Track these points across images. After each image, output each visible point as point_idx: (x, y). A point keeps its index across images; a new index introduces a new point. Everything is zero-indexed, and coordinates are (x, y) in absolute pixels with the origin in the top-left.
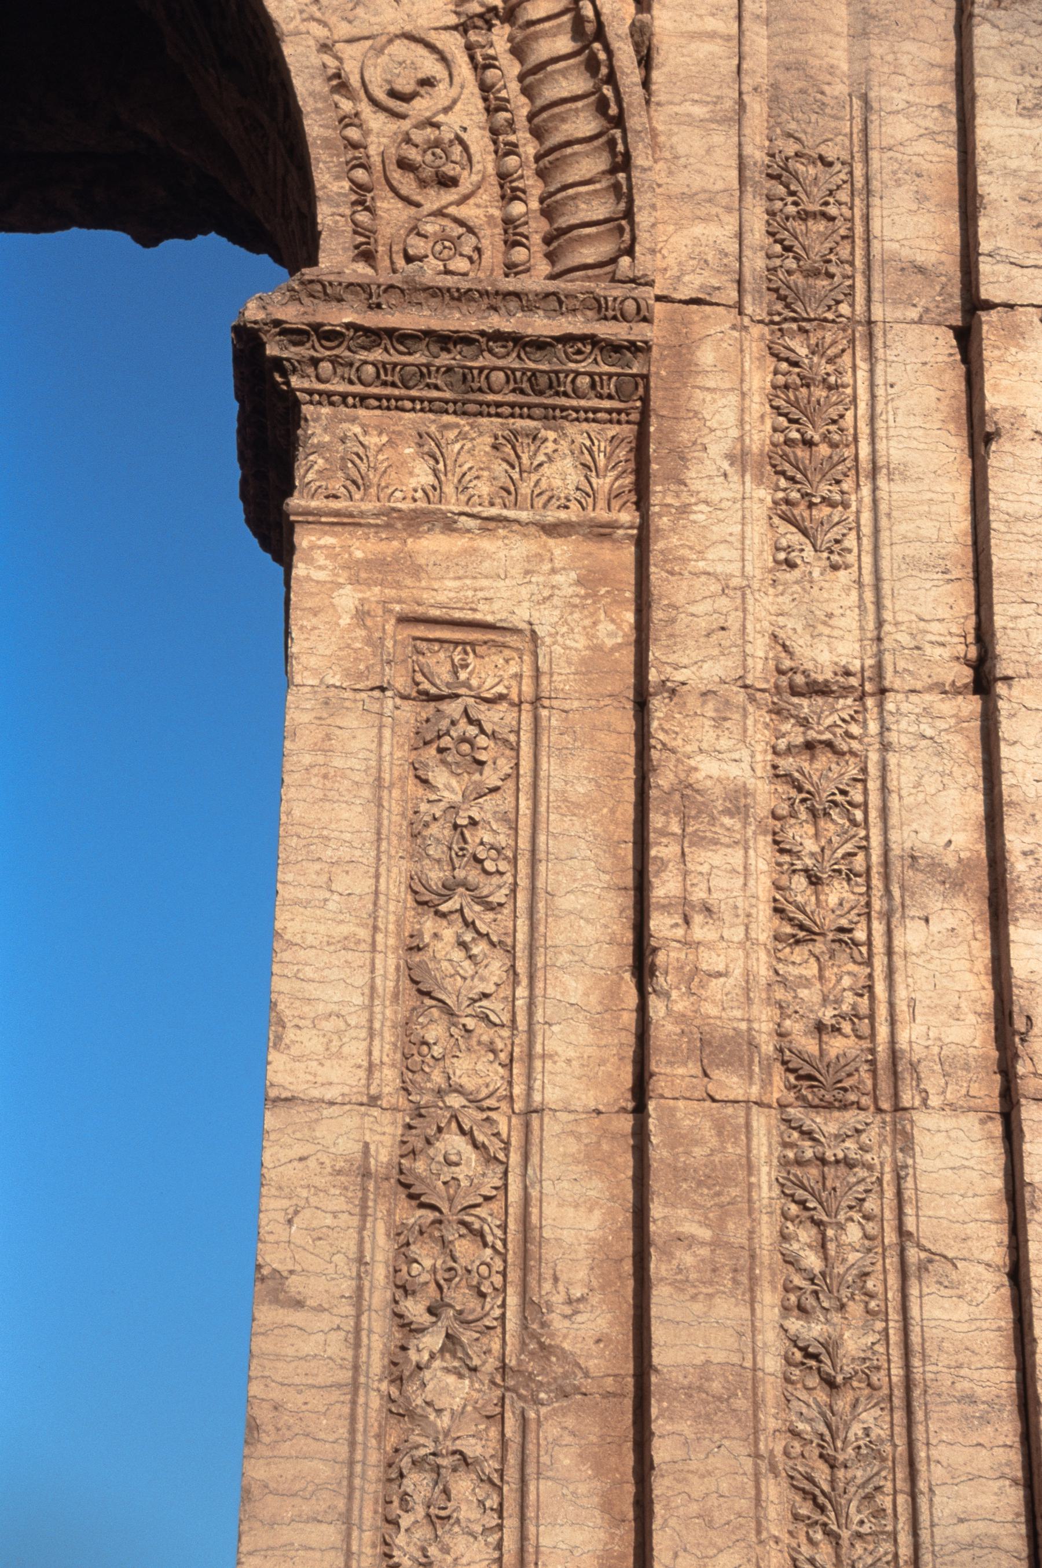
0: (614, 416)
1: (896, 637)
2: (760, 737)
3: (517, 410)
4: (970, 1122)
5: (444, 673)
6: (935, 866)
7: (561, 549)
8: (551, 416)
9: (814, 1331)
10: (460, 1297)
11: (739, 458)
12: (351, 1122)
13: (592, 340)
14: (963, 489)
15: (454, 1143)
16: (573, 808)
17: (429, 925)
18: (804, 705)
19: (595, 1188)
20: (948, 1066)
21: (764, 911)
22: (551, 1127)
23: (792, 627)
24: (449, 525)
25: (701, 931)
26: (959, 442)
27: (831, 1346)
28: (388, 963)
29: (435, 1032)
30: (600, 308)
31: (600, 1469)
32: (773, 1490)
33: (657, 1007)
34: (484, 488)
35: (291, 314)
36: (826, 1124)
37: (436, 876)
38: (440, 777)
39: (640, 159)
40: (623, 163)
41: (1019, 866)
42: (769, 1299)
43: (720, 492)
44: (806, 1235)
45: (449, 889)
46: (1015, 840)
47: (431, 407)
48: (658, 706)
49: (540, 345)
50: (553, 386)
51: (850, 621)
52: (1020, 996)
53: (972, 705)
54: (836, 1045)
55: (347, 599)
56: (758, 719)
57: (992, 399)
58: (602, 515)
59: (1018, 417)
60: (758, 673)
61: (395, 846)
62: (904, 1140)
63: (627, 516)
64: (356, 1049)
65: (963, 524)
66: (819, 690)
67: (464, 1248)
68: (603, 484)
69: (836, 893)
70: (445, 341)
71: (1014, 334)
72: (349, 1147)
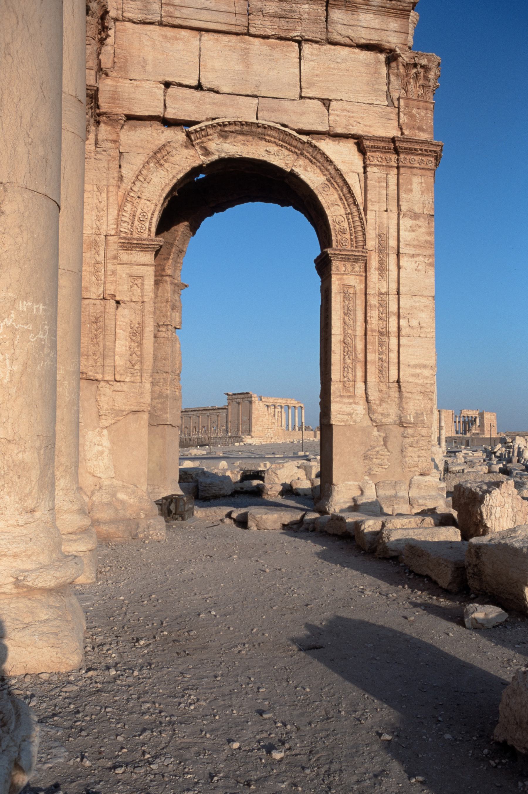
0: (363, 263)
1: (390, 289)
2: (377, 299)
3: (353, 262)
4: (395, 338)
5: (346, 290)
6: (393, 313)
7: (357, 277)
8: (356, 262)
9: (381, 357)
10: (349, 353)
11: (376, 269)
12: (339, 336)
13: (362, 255)
14: (397, 273)
15: (349, 338)
16: (359, 305)
17: (346, 317)
18: (381, 296)
19: (361, 343)
20: (393, 333)
21: (377, 317)
22: (357, 337)
23: (380, 287)
24: (347, 274)
25: (372, 319)
26: (396, 268)
27: (382, 358)
28: (342, 321)
29: (346, 328)
30: (363, 252)
31: (362, 368)
32: (377, 371)
33: (368, 327)
34: (350, 270)
35: (332, 252)
36: (382, 338)
37: (346, 312)
38: (346, 302)
39: (367, 235)
40: (364, 234)
41: (401, 314)
42: (377, 354)
43: (374, 273)
44: (380, 348)
45: (347, 313)
46: (401, 311)
47: (345, 261)
48: (368, 296)
49: (356, 256)
50: (357, 259)
51: (385, 287)
52: (401, 327)
53: (397, 296)
54: (383, 330)
55: (337, 283)
56: (377, 297)
57: (401, 264)
58: (361, 274)
59: (403, 266)
60: (377, 292)
61: (342, 309)
62: (389, 339)
63: (364, 274)
64: (339, 329)
65: (397, 276)
66: (382, 294)
67: (350, 348)
68: (361, 270)
69: (384, 315)
70: (347, 255)
71: (403, 256)
72: (339, 339)
